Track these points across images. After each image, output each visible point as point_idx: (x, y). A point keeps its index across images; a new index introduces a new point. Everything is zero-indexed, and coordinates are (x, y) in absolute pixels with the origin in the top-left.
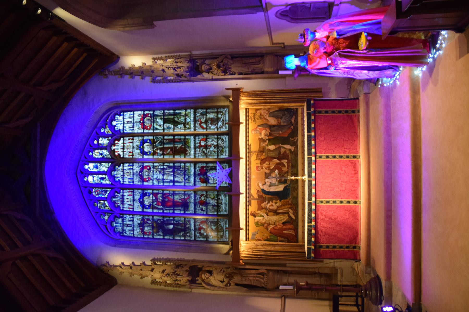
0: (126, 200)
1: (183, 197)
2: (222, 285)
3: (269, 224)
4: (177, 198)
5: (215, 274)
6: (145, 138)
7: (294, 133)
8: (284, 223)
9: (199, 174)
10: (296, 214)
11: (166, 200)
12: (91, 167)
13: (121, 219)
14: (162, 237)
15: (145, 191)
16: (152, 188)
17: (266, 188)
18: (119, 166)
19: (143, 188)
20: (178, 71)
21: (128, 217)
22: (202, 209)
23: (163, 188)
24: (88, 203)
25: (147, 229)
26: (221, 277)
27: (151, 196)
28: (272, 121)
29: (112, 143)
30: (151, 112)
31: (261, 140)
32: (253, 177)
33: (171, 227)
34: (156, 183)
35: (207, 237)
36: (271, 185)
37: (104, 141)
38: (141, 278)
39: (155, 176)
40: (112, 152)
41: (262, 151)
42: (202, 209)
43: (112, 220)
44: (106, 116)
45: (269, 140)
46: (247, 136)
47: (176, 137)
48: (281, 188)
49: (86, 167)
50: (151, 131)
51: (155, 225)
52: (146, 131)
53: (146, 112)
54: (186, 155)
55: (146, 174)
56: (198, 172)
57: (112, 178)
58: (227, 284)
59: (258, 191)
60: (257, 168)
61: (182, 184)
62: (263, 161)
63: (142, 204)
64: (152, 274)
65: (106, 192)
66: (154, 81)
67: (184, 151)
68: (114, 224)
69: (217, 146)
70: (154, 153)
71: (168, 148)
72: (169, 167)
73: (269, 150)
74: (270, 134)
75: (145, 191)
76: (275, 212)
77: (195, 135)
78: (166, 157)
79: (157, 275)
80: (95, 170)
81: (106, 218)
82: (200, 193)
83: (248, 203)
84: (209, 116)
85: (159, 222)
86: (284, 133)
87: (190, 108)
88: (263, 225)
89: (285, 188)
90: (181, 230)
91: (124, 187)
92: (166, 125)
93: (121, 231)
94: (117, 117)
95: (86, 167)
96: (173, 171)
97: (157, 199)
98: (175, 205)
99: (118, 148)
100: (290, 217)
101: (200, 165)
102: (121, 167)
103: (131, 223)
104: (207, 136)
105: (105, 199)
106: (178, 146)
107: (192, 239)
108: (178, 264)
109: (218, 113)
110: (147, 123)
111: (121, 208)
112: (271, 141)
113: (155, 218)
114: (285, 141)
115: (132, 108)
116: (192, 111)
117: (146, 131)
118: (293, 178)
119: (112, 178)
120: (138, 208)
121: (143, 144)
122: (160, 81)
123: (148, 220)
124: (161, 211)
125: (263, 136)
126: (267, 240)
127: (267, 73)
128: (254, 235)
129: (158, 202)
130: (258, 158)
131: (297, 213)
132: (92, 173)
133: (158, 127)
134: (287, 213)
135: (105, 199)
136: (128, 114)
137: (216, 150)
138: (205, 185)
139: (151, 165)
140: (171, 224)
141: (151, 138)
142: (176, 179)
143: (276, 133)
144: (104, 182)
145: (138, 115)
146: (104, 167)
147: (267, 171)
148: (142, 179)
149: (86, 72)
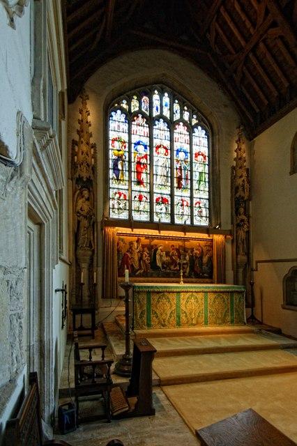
0: (141, 128)
1: (145, 181)
2: (78, 208)
3: (131, 253)
4: (144, 176)
5: (87, 203)
6: (189, 154)
7: (197, 276)
8: (132, 265)
9: (162, 198)
10: (140, 276)
11: (142, 166)
12: (166, 99)
13: (124, 120)
14: (110, 157)
15: (148, 148)
16: (151, 156)
17: (159, 251)
18: (168, 127)
19: (151, 146)
20: (241, 189)
21: (126, 127)
22: (135, 197)
23: (151, 164)
24: (138, 90)
25: (117, 145)
26: (86, 207)
27: (145, 153)
28: (205, 259)
29: (185, 124)
31: (192, 250)
32: (167, 242)
33: (120, 167)
34: (155, 159)
35: (113, 199)
36: (161, 256)
37: (186, 116)
39: (160, 159)
40: (177, 122)
41: (185, 250)
42: (135, 197)
43: (123, 111)
44: (206, 122)
45: (192, 256)
46: (195, 239)
47: (189, 181)
48: (159, 264)
49: (166, 94)
50: (194, 161)
51: (121, 152)
52: (194, 156)
54: (177, 188)
55: (162, 150)
56: (164, 196)
57: (158, 118)
58: (80, 214)
59: (156, 245)
60: (173, 246)
61: (154, 182)
62: (178, 250)
63: (138, 143)
64: (84, 142)
65: (146, 110)
67: (179, 187)
68: (119, 112)
69: (183, 215)
70: (178, 161)
71: (181, 173)
72: (167, 172)
73: (186, 256)
74: (196, 257)
75: (148, 148)
76: (140, 259)
77: (191, 197)
78: (175, 170)
79: (84, 148)
80: (164, 105)
81: (124, 106)
82: (148, 197)
83: (147, 237)
84: (204, 210)
85: (124, 157)
86: (197, 269)
87: (209, 195)
88: (131, 248)
89: (158, 268)
90: (117, 176)
92: (198, 174)
93: (114, 118)
94: (204, 132)
95: (166, 94)
96: (164, 176)
97: (142, 158)
98: (139, 173)
99: (181, 128)
100: (138, 270)
101: (169, 199)
102: (166, 129)
103: (121, 130)
104: (191, 207)
105: (140, 107)
106: (183, 182)
107: (111, 186)
108: (94, 169)
109: (206, 217)
110: (200, 157)
111: (133, 123)
112: (191, 258)
113: (127, 154)
114: (192, 268)
115: (212, 146)
116: (207, 197)
117: (194, 156)
118: (182, 274)
119: (158, 118)
120: (135, 139)
121: (185, 152)
122: (233, 173)
123: (125, 148)
124: (133, 160)
125: (195, 251)
126: (118, 251)
127: (237, 257)
128: (123, 240)
129: (140, 158)
130: (180, 246)
131: (140, 277)
132: (161, 100)
133: (196, 167)
134: (140, 268)
135: (140, 107)
136: (205, 141)
137: (180, 213)
138: (155, 201)
139: (169, 157)
140: (123, 168)
141: (189, 160)
142: (159, 177)
143: (197, 262)
144: (154, 109)
145: (205, 151)
146: (166, 113)
147: (171, 254)
148: (158, 147)
149: (243, 107)
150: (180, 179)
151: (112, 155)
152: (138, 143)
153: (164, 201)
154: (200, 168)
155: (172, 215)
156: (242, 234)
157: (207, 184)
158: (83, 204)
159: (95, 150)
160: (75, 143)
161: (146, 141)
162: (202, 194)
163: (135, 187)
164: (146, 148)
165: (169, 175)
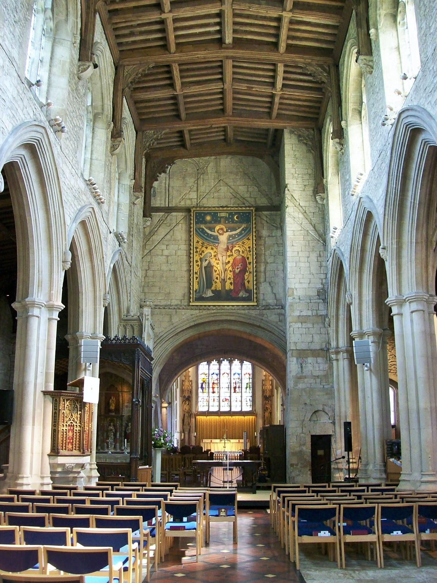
4: (216, 390)
6: (240, 375)
16: (219, 378)
19: (219, 374)
26: (187, 409)
30: (251, 377)
33: (204, 386)
38: (184, 376)
53: (251, 375)
55: (226, 375)
66: (263, 380)
67: (235, 392)
79: (187, 383)
90: (203, 391)
91: (220, 365)
98: (213, 388)
106: (237, 389)
108: (191, 392)
116: (251, 395)
120: (211, 372)
122: (263, 383)
150: (235, 388)
151: (200, 381)
152: (213, 374)
153: (226, 400)
154: (247, 380)
155: (230, 406)
156: (267, 414)
157: (251, 389)
158: (186, 407)
159: (192, 383)
160: (183, 381)
161: (217, 372)
162: (248, 394)
163: (211, 395)
164: (217, 375)
165: (229, 387)
